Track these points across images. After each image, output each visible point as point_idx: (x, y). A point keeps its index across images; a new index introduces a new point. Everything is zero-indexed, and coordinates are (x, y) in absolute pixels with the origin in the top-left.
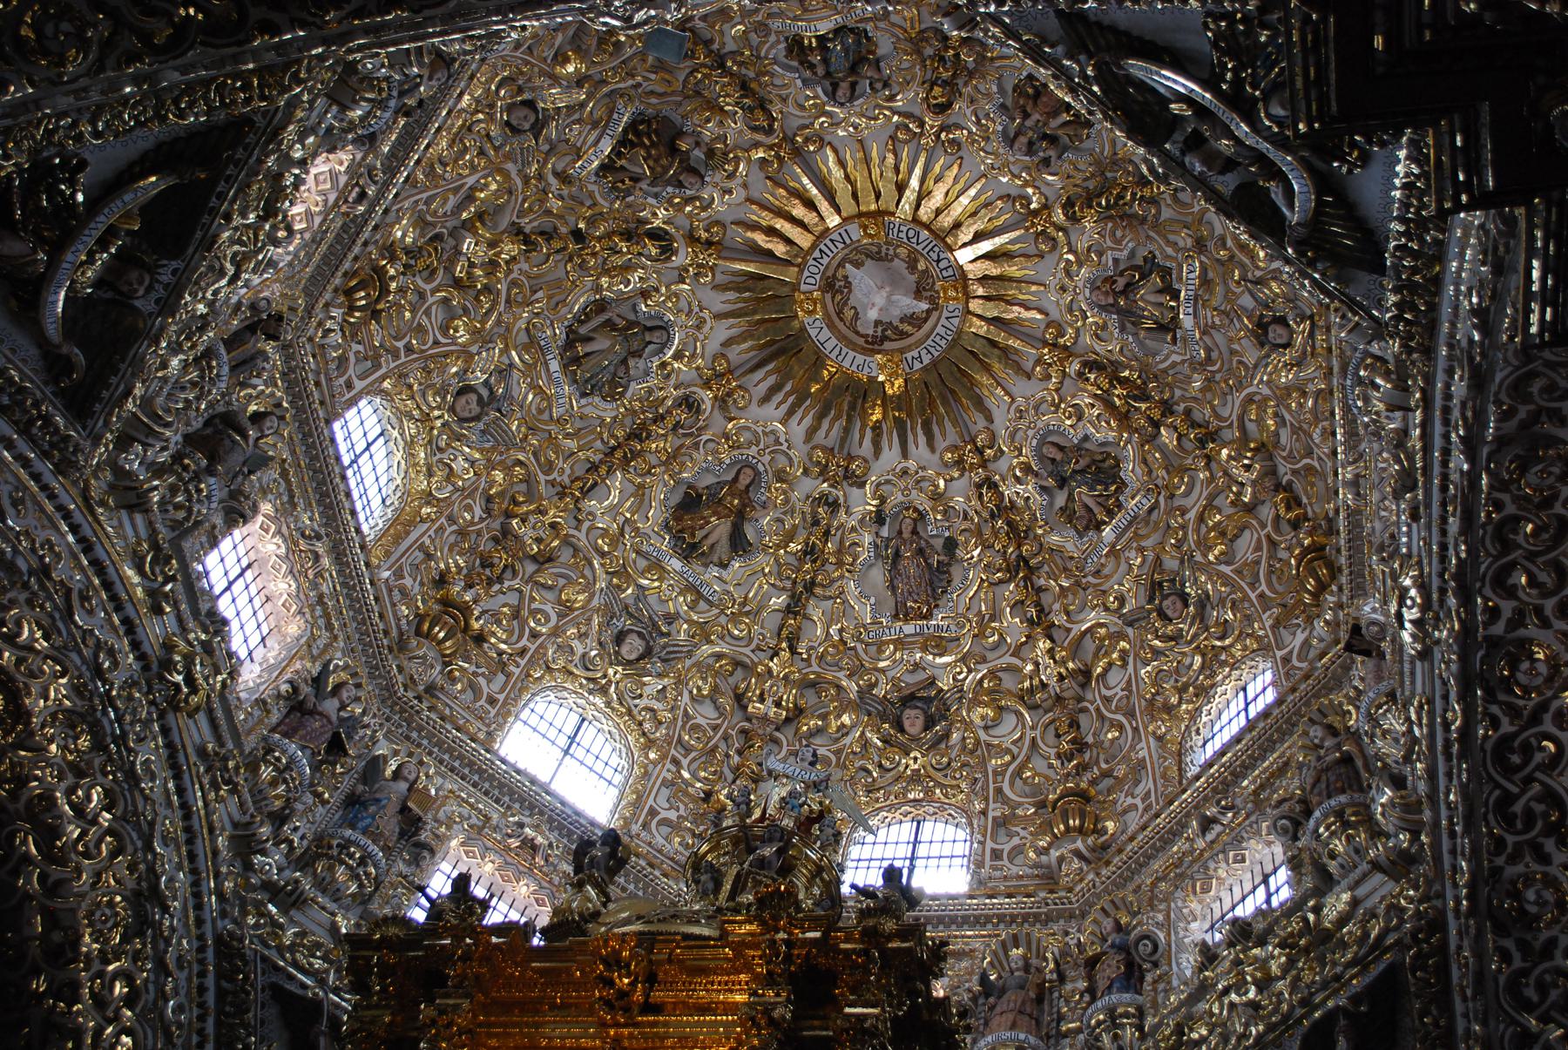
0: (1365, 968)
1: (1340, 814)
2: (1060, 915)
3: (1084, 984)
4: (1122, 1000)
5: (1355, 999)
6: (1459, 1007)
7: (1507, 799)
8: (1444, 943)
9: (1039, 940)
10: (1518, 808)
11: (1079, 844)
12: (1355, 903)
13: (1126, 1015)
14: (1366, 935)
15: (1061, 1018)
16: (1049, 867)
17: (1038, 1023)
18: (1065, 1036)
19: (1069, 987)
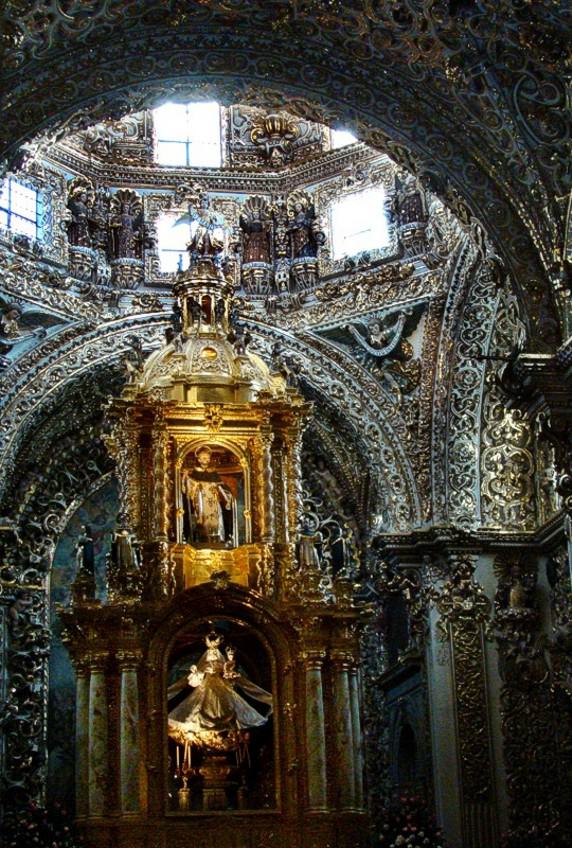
0: (416, 301)
1: (413, 231)
2: (272, 182)
3: (285, 230)
4: (309, 259)
5: (408, 310)
6: (444, 322)
7: (480, 288)
8: (444, 304)
9: (265, 202)
10: (483, 291)
11: (281, 144)
12: (413, 269)
13: (311, 268)
14: (416, 290)
15: (276, 246)
16: (265, 151)
17: (269, 251)
18: (279, 257)
19: (279, 230)
